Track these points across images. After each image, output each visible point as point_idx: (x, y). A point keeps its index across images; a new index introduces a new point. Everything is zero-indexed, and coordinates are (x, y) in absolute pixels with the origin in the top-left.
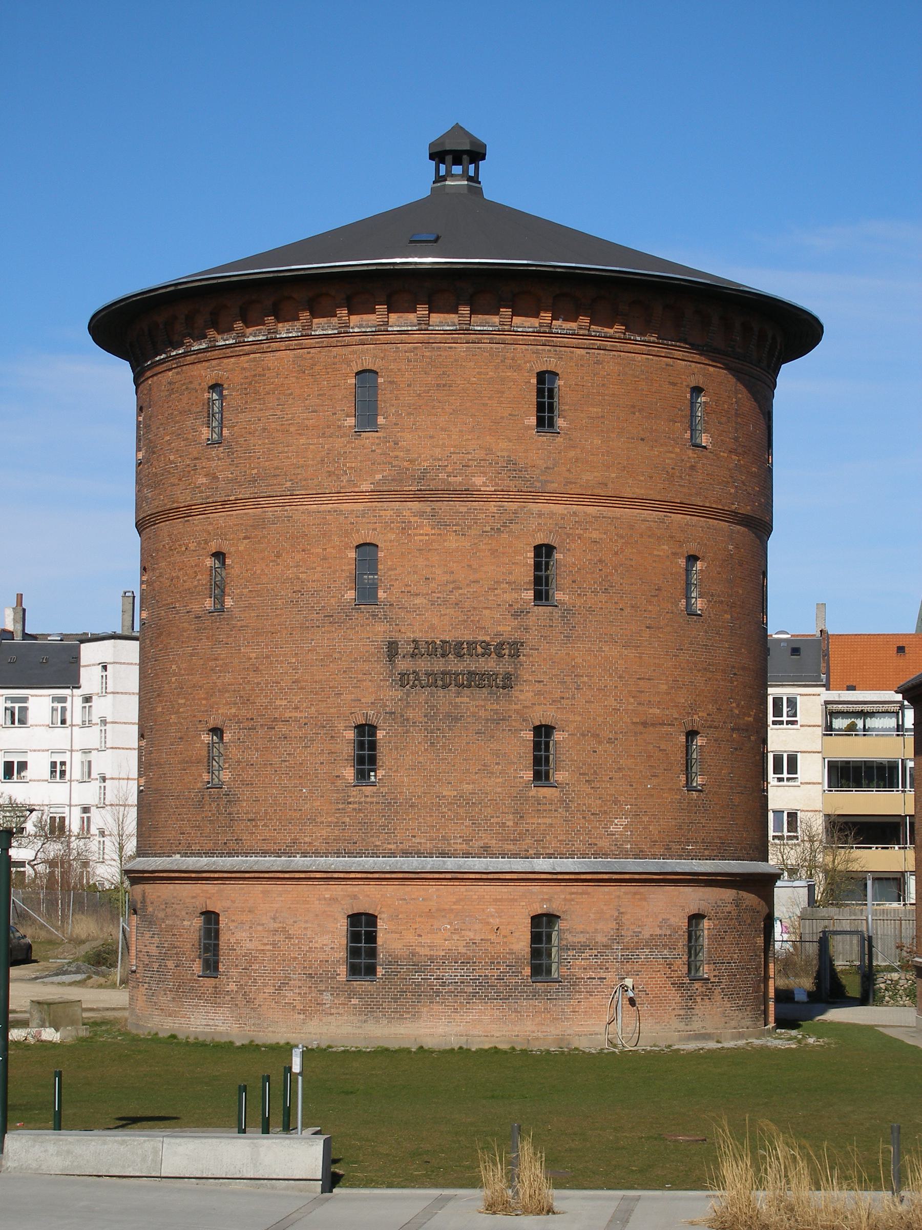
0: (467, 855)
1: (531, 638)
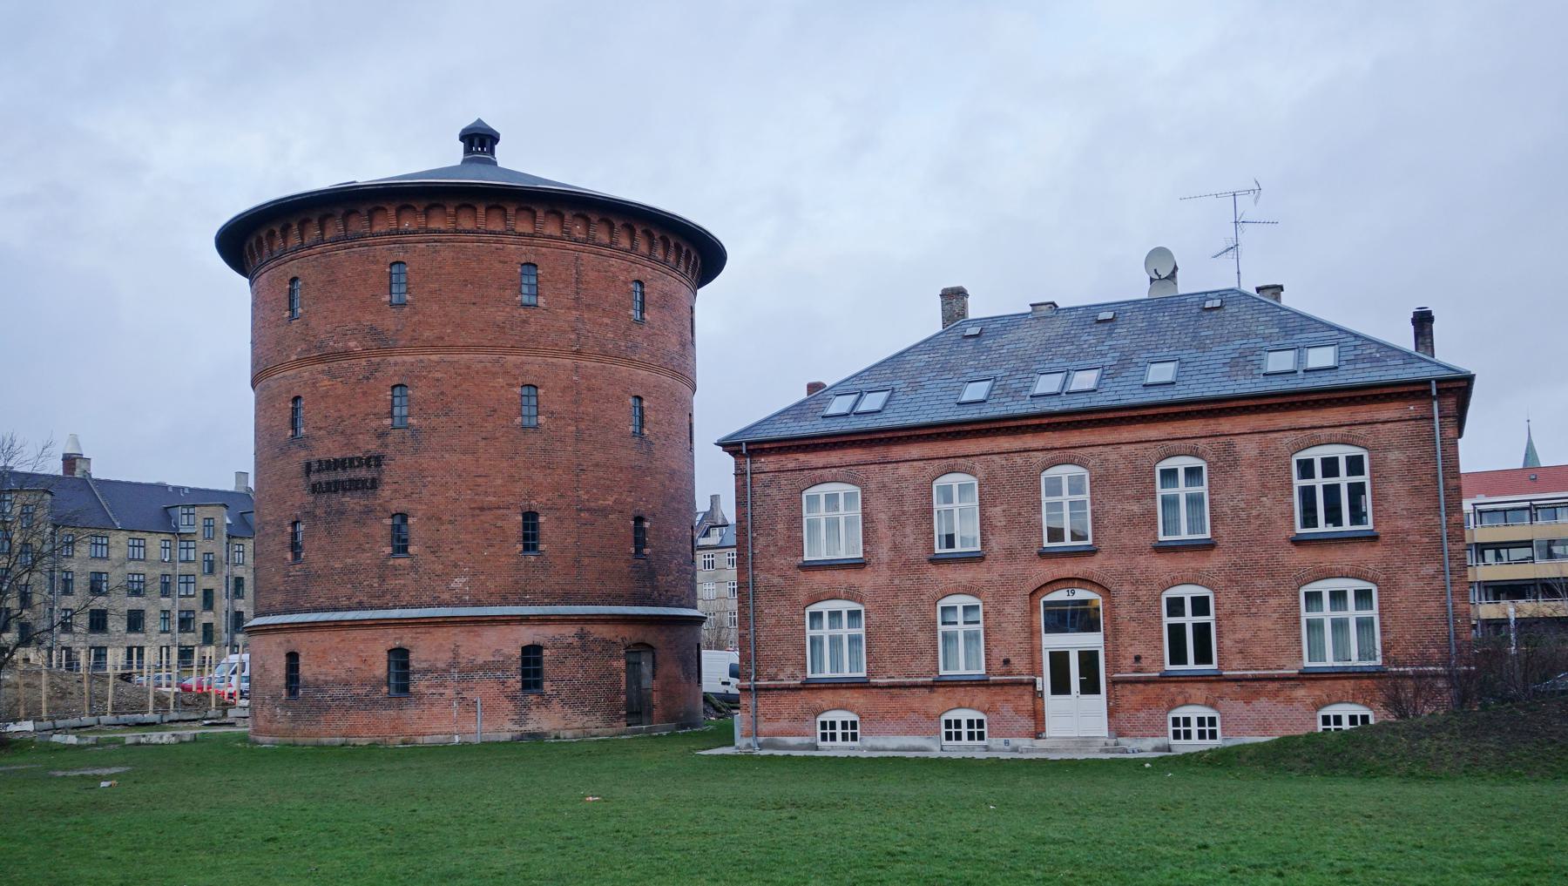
0: (349, 609)
1: (389, 451)
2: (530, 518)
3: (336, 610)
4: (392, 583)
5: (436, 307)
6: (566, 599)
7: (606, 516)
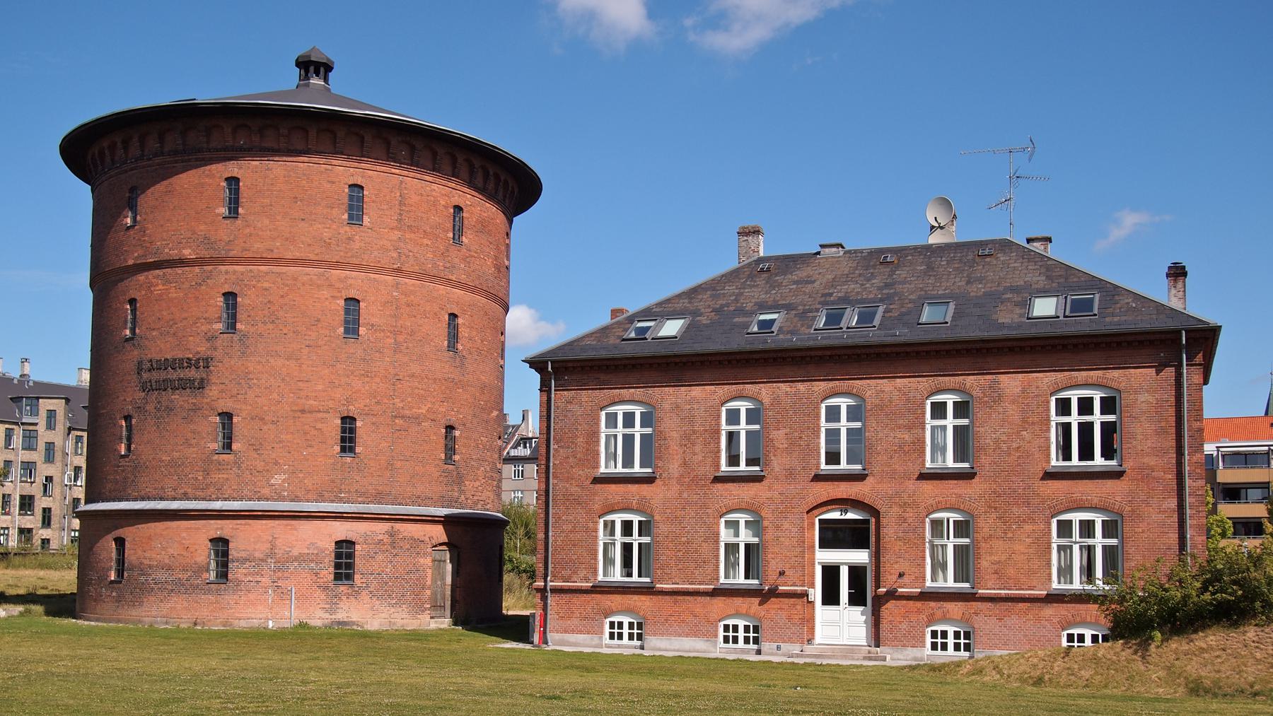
0: (174, 499)
1: (218, 354)
2: (348, 422)
3: (162, 499)
4: (217, 477)
5: (267, 222)
6: (379, 498)
7: (419, 424)
